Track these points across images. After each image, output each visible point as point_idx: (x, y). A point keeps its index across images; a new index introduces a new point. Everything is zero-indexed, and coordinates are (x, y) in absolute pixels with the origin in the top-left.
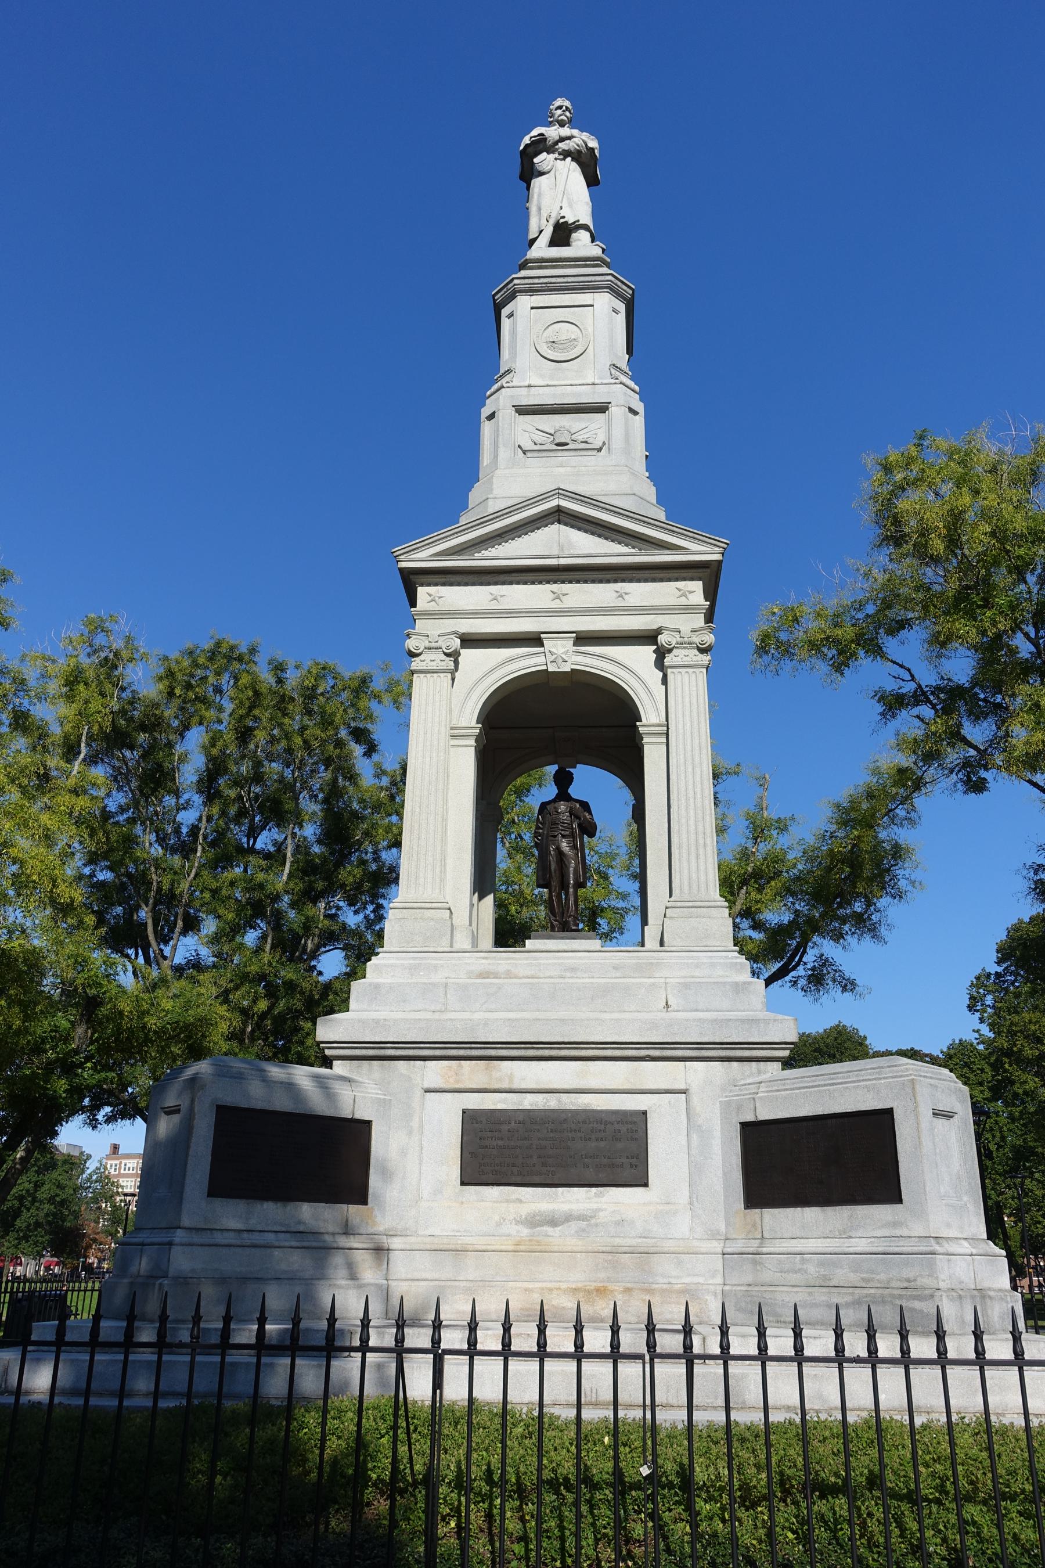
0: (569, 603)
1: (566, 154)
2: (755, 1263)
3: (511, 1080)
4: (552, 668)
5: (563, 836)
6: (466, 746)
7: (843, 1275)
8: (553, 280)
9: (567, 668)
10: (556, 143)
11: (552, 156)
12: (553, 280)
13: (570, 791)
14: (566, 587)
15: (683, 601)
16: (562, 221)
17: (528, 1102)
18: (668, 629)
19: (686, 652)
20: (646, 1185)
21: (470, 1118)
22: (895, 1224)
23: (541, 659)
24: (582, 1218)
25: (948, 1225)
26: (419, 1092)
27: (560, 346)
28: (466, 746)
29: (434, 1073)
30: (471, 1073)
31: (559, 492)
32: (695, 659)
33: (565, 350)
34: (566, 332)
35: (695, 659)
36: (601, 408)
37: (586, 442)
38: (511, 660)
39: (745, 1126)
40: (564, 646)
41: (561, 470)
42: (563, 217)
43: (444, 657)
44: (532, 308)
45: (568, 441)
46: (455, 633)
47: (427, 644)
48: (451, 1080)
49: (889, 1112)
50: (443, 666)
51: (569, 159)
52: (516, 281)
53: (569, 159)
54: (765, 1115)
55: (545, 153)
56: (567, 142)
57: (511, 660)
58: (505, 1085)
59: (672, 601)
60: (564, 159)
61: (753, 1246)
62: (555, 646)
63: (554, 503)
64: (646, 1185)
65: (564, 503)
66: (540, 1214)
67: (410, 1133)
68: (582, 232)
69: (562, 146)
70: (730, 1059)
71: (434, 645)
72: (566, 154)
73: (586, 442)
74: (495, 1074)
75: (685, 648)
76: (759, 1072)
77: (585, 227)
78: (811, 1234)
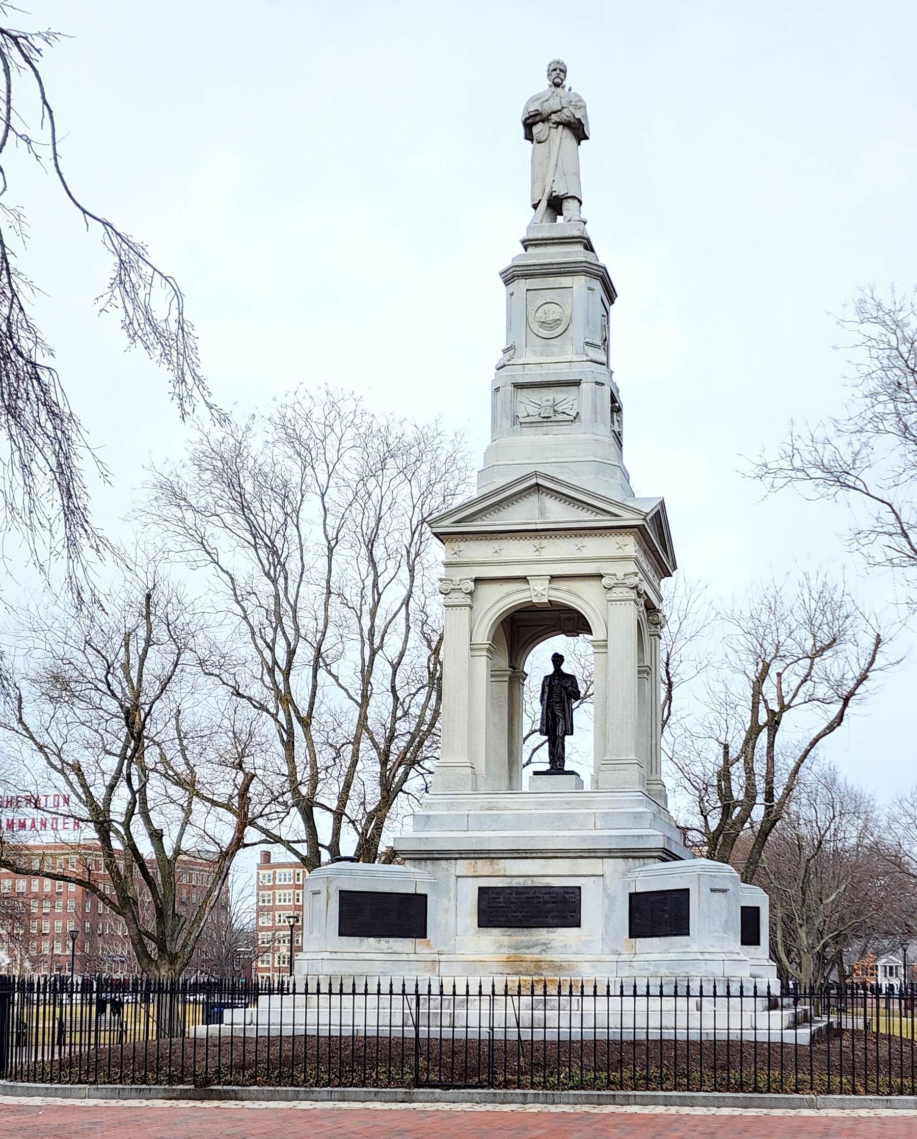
1: (558, 124)
2: (630, 966)
3: (505, 871)
5: (557, 703)
7: (663, 971)
10: (550, 115)
11: (546, 125)
13: (562, 667)
14: (544, 542)
16: (554, 194)
17: (515, 883)
20: (579, 926)
21: (481, 890)
22: (687, 946)
23: (527, 594)
24: (544, 944)
25: (712, 946)
26: (453, 878)
29: (462, 867)
30: (483, 867)
31: (536, 474)
32: (626, 595)
33: (552, 328)
34: (553, 313)
35: (626, 595)
36: (577, 383)
37: (564, 413)
38: (508, 595)
39: (631, 894)
40: (542, 585)
43: (463, 595)
44: (528, 290)
45: (551, 414)
47: (452, 586)
48: (472, 871)
49: (688, 890)
51: (561, 127)
53: (561, 127)
54: (640, 890)
55: (541, 124)
57: (508, 595)
58: (502, 873)
60: (557, 128)
61: (630, 958)
62: (536, 585)
63: (533, 481)
64: (579, 926)
65: (540, 482)
66: (522, 941)
67: (449, 900)
68: (570, 200)
69: (554, 117)
70: (627, 857)
71: (456, 587)
72: (558, 124)
73: (564, 413)
74: (496, 867)
76: (644, 864)
78: (657, 951)
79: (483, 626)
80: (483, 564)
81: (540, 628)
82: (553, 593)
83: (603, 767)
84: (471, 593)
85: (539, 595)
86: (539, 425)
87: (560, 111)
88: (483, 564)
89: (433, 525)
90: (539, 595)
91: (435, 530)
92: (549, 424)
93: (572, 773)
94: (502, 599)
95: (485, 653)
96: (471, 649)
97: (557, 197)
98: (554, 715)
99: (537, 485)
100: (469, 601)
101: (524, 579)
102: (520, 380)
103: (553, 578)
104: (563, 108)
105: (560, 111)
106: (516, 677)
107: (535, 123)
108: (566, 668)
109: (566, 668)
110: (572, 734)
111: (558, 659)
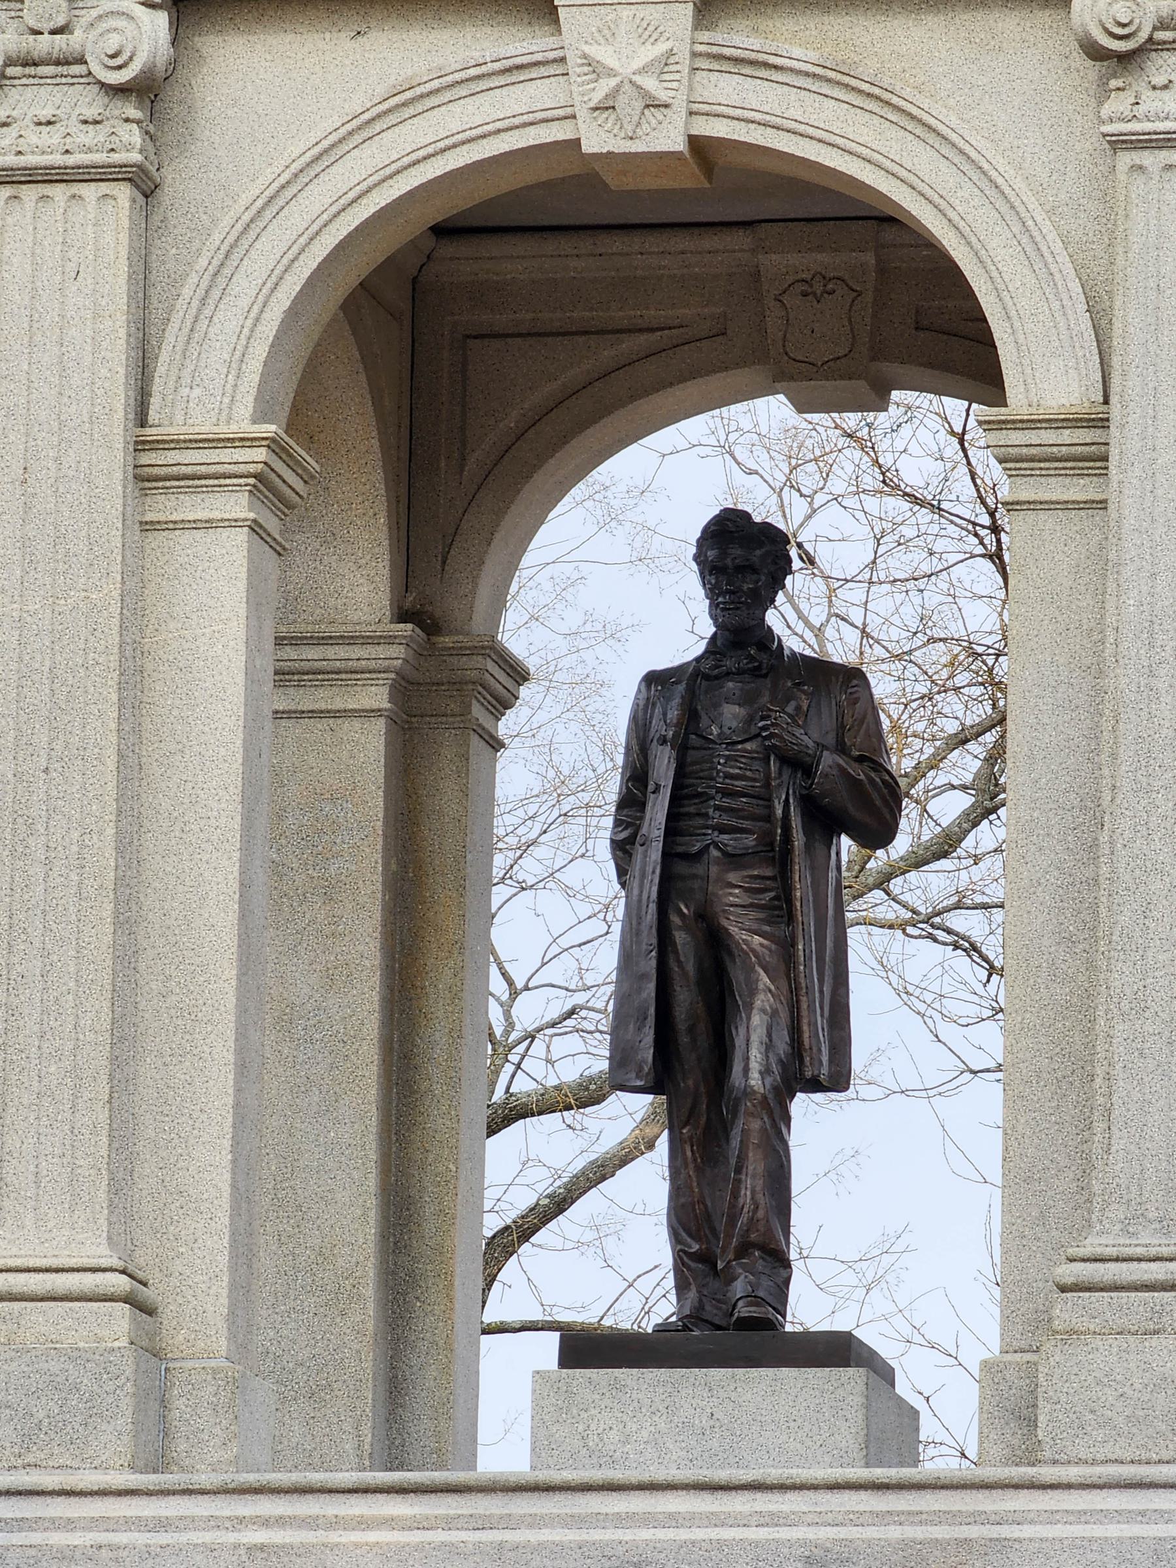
4: (597, 140)
5: (734, 860)
9: (668, 137)
38: (408, 101)
43: (90, 103)
50: (88, 146)
62: (609, 35)
71: (45, 44)
79: (228, 321)
81: (608, 353)
82: (725, 88)
83: (1066, 1311)
84: (148, 91)
90: (630, 106)
93: (836, 1350)
94: (364, 127)
96: (145, 481)
98: (715, 943)
100: (127, 141)
106: (448, 689)
108: (796, 620)
109: (796, 620)
110: (837, 1080)
111: (743, 558)
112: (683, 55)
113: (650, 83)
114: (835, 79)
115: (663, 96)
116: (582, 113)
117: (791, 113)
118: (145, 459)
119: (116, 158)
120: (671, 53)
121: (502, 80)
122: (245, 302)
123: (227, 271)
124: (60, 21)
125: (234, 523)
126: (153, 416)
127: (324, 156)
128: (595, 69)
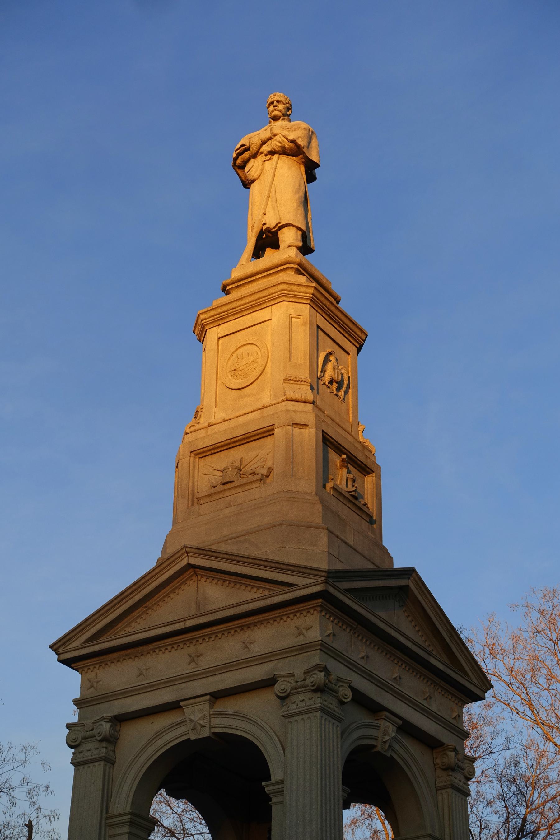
0: (205, 663)
1: (272, 153)
4: (193, 737)
6: (121, 834)
8: (234, 305)
9: (206, 733)
11: (260, 158)
12: (234, 305)
14: (202, 647)
15: (301, 640)
16: (264, 228)
18: (283, 676)
19: (301, 697)
27: (241, 373)
28: (121, 834)
41: (227, 511)
42: (264, 224)
46: (103, 718)
52: (202, 317)
56: (269, 142)
57: (159, 734)
59: (291, 642)
63: (184, 562)
65: (193, 561)
68: (284, 230)
71: (89, 733)
72: (272, 153)
75: (301, 693)
77: (288, 225)
80: (125, 693)
82: (217, 721)
85: (199, 727)
86: (221, 496)
87: (271, 138)
88: (125, 693)
89: (60, 650)
91: (63, 657)
92: (233, 491)
94: (151, 742)
95: (126, 829)
97: (268, 230)
99: (190, 566)
101: (174, 706)
102: (201, 445)
103: (217, 696)
104: (275, 135)
105: (271, 138)
107: (246, 162)
112: (208, 715)
113: (201, 722)
114: (236, 715)
115: (204, 724)
116: (190, 731)
117: (230, 724)
118: (108, 821)
119: (100, 755)
120: (205, 715)
121: (176, 727)
122: (128, 784)
123: (125, 778)
124: (91, 728)
125: (126, 833)
126: (110, 812)
127: (143, 749)
128: (191, 721)
